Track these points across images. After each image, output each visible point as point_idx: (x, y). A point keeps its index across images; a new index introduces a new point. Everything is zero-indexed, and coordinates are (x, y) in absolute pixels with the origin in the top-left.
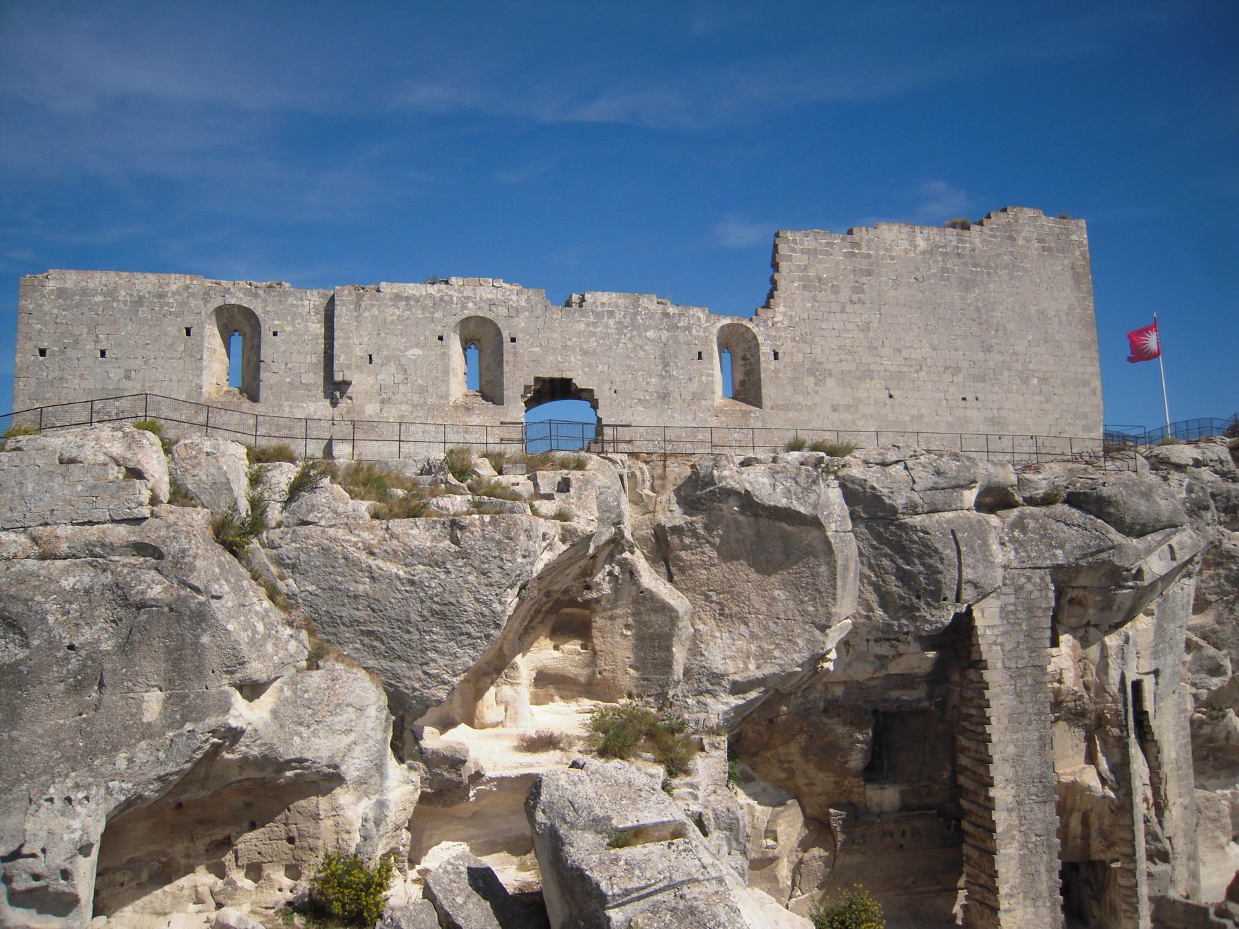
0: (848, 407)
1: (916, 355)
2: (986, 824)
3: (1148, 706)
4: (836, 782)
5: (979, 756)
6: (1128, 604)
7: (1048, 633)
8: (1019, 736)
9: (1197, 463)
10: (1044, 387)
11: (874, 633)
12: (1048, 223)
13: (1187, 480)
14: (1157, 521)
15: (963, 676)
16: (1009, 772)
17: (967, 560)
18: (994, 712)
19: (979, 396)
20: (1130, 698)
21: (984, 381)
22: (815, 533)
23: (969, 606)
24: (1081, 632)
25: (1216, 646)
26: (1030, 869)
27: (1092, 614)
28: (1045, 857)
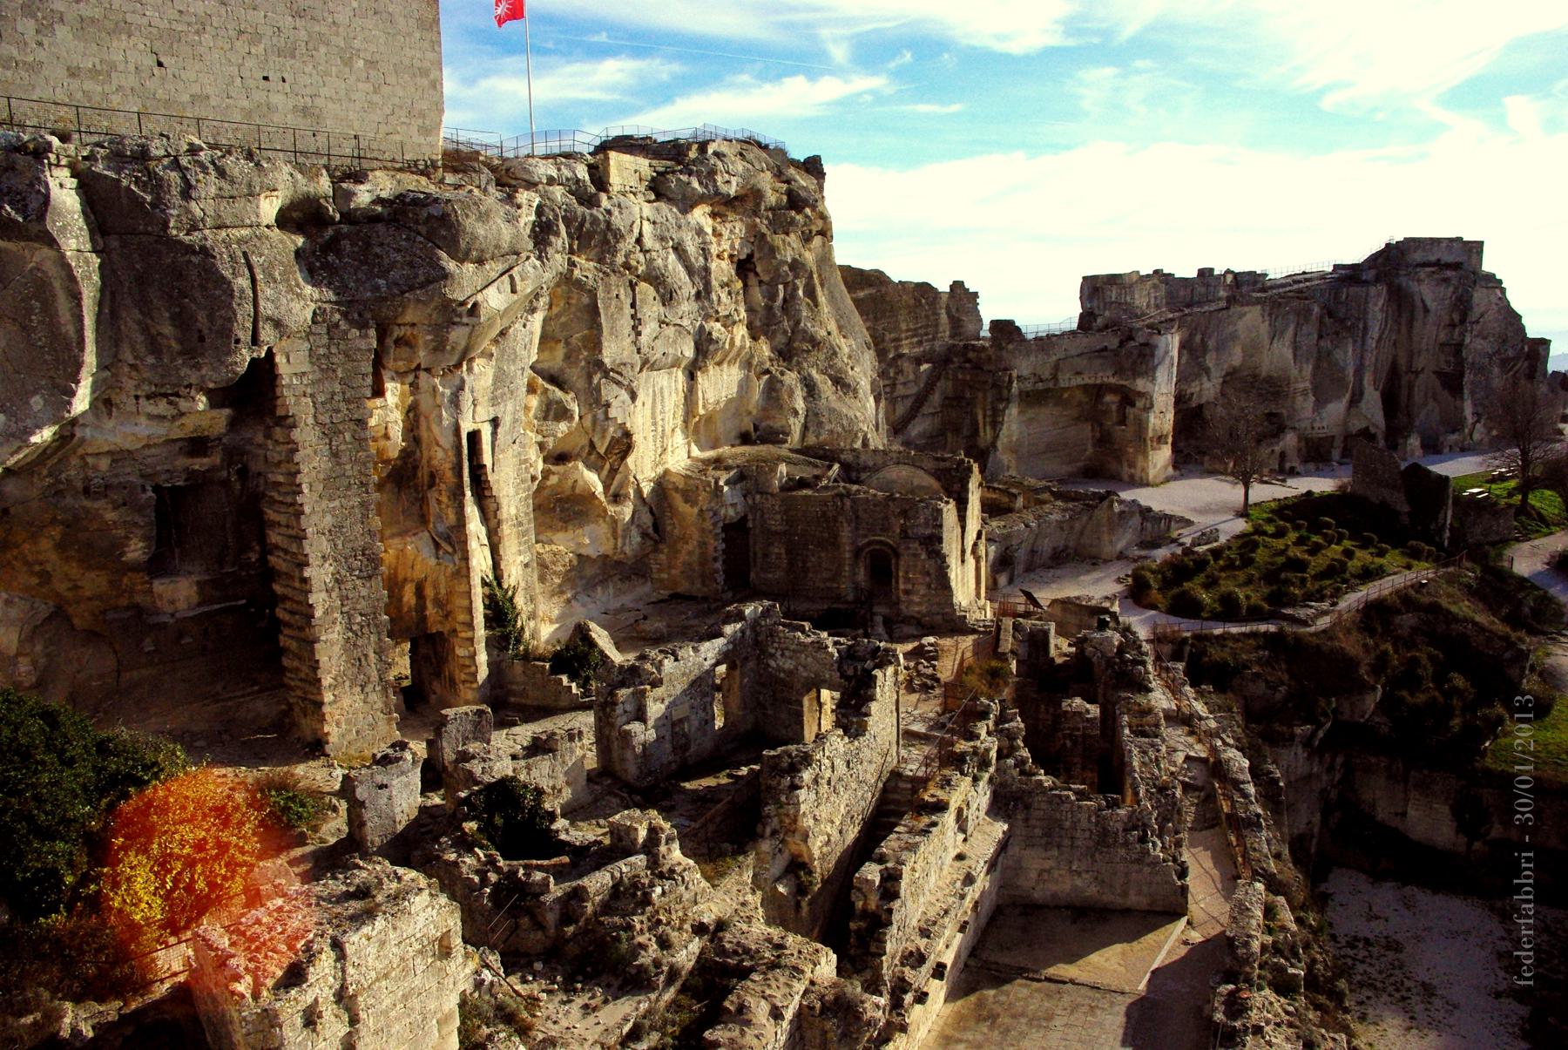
2: (304, 609)
3: (487, 459)
4: (110, 582)
5: (291, 532)
6: (463, 344)
7: (369, 380)
8: (337, 503)
9: (551, 181)
10: (372, 73)
11: (146, 387)
13: (537, 200)
14: (497, 247)
15: (268, 436)
16: (325, 545)
17: (266, 291)
18: (304, 480)
19: (286, 76)
20: (465, 451)
21: (294, 57)
22: (46, 252)
23: (270, 349)
24: (411, 378)
25: (561, 388)
26: (357, 653)
27: (422, 356)
28: (373, 638)
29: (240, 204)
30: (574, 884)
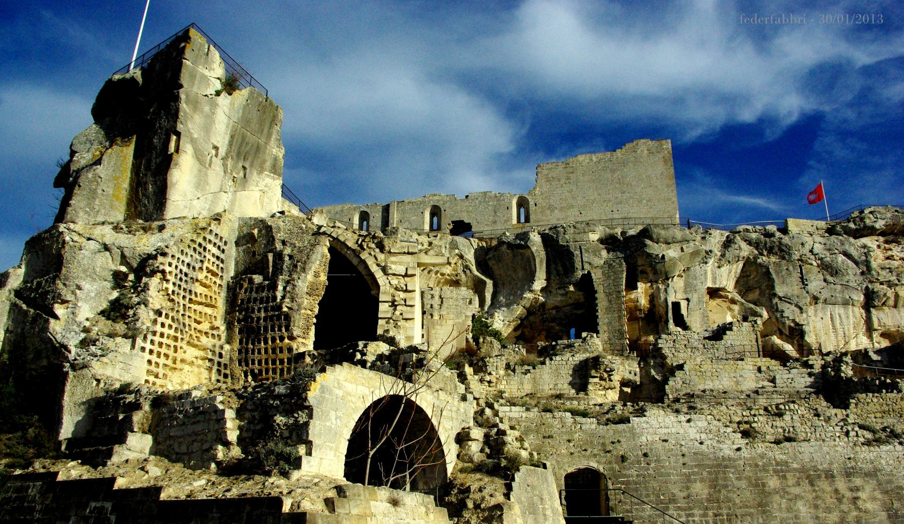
0: (563, 219)
1: (592, 198)
3: (684, 311)
12: (650, 143)
16: (605, 328)
17: (585, 255)
18: (599, 308)
29: (581, 235)
30: (483, 278)
